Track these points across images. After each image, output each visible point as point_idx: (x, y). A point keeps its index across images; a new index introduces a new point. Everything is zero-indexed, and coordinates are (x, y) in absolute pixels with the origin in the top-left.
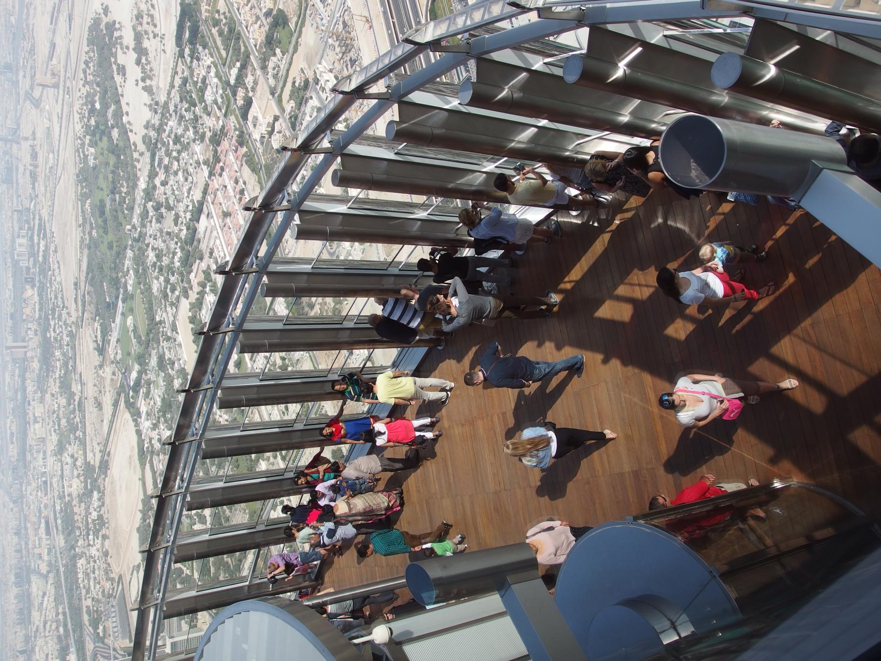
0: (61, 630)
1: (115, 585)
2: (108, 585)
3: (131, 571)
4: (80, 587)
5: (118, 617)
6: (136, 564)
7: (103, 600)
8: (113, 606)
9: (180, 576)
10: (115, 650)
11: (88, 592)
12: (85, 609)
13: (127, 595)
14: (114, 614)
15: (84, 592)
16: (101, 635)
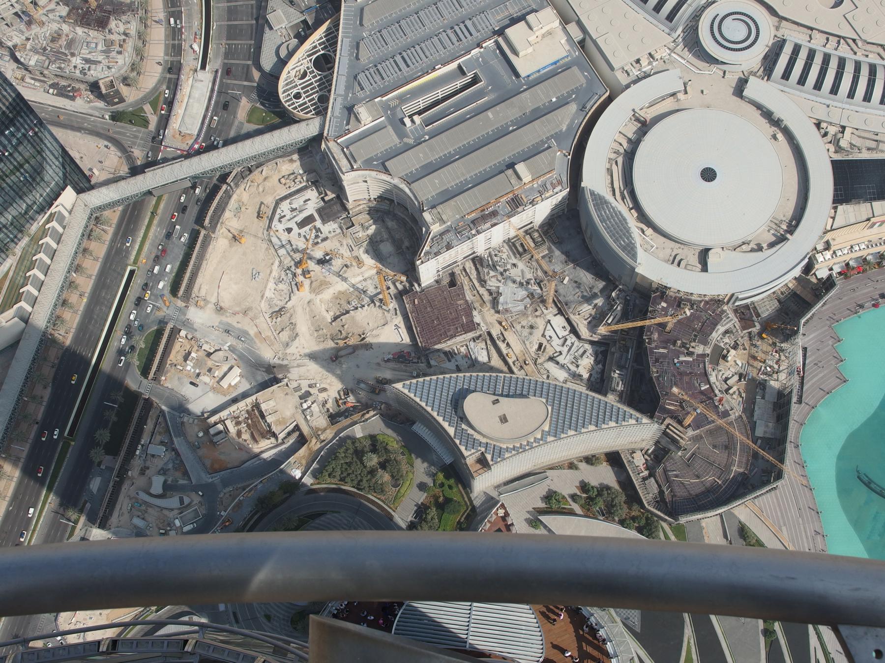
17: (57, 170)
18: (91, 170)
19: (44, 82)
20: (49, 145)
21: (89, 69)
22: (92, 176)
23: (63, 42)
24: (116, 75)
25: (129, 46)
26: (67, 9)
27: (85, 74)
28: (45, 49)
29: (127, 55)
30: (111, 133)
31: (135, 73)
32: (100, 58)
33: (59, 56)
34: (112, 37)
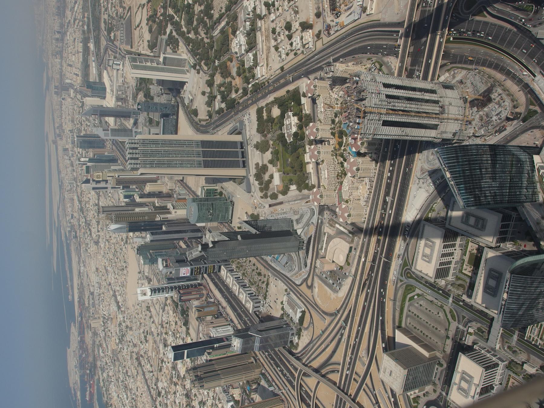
0: (86, 27)
1: (126, 12)
2: (121, 10)
3: (138, 7)
4: (101, 6)
5: (124, 31)
6: (142, 3)
7: (116, 18)
8: (122, 24)
9: (172, 19)
10: (120, 49)
11: (106, 10)
12: (103, 20)
13: (133, 20)
14: (122, 29)
15: (103, 10)
16: (112, 38)
17: (524, 154)
18: (534, 144)
19: (492, 134)
20: (513, 150)
21: (501, 116)
22: (537, 145)
23: (485, 117)
24: (510, 109)
25: (504, 96)
26: (475, 108)
27: (501, 119)
28: (482, 125)
29: (507, 100)
30: (528, 127)
31: (515, 102)
32: (500, 110)
33: (488, 123)
34: (497, 100)
